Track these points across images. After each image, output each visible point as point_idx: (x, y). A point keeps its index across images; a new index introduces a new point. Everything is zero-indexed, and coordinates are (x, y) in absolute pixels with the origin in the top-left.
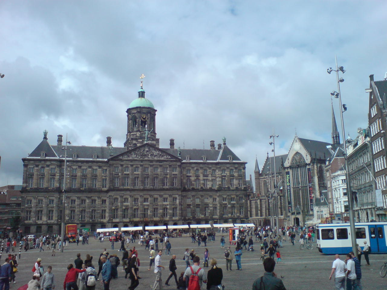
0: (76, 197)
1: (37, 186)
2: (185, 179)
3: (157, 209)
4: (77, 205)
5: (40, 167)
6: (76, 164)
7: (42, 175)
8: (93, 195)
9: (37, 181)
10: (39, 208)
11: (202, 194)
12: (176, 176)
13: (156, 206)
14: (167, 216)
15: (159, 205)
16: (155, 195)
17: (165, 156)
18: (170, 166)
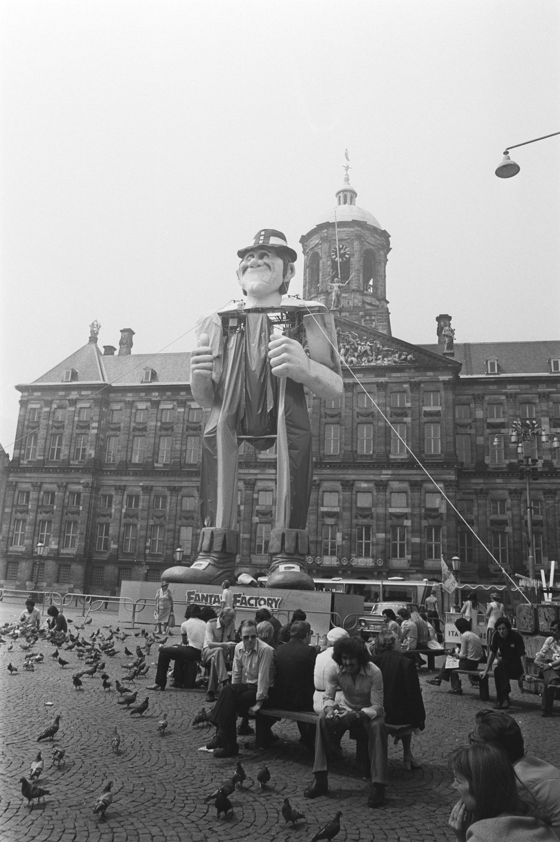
0: (140, 486)
1: (44, 456)
2: (482, 435)
3: (368, 528)
4: (143, 510)
5: (54, 406)
6: (146, 395)
7: (58, 428)
8: (184, 484)
9: (46, 442)
10: (44, 514)
11: (548, 486)
12: (436, 418)
13: (365, 517)
14: (402, 556)
15: (375, 515)
16: (358, 480)
17: (397, 355)
18: (415, 386)
